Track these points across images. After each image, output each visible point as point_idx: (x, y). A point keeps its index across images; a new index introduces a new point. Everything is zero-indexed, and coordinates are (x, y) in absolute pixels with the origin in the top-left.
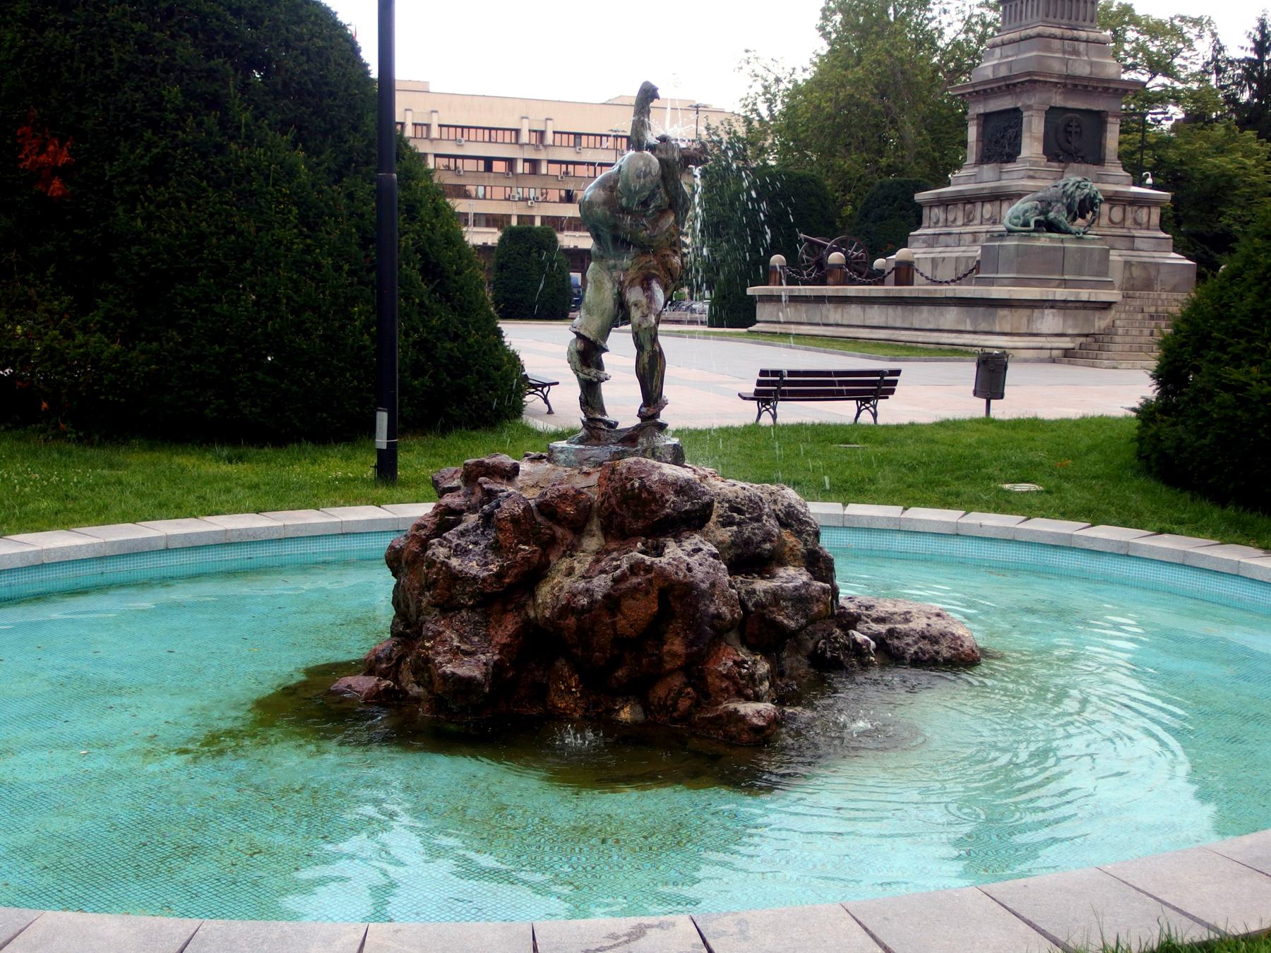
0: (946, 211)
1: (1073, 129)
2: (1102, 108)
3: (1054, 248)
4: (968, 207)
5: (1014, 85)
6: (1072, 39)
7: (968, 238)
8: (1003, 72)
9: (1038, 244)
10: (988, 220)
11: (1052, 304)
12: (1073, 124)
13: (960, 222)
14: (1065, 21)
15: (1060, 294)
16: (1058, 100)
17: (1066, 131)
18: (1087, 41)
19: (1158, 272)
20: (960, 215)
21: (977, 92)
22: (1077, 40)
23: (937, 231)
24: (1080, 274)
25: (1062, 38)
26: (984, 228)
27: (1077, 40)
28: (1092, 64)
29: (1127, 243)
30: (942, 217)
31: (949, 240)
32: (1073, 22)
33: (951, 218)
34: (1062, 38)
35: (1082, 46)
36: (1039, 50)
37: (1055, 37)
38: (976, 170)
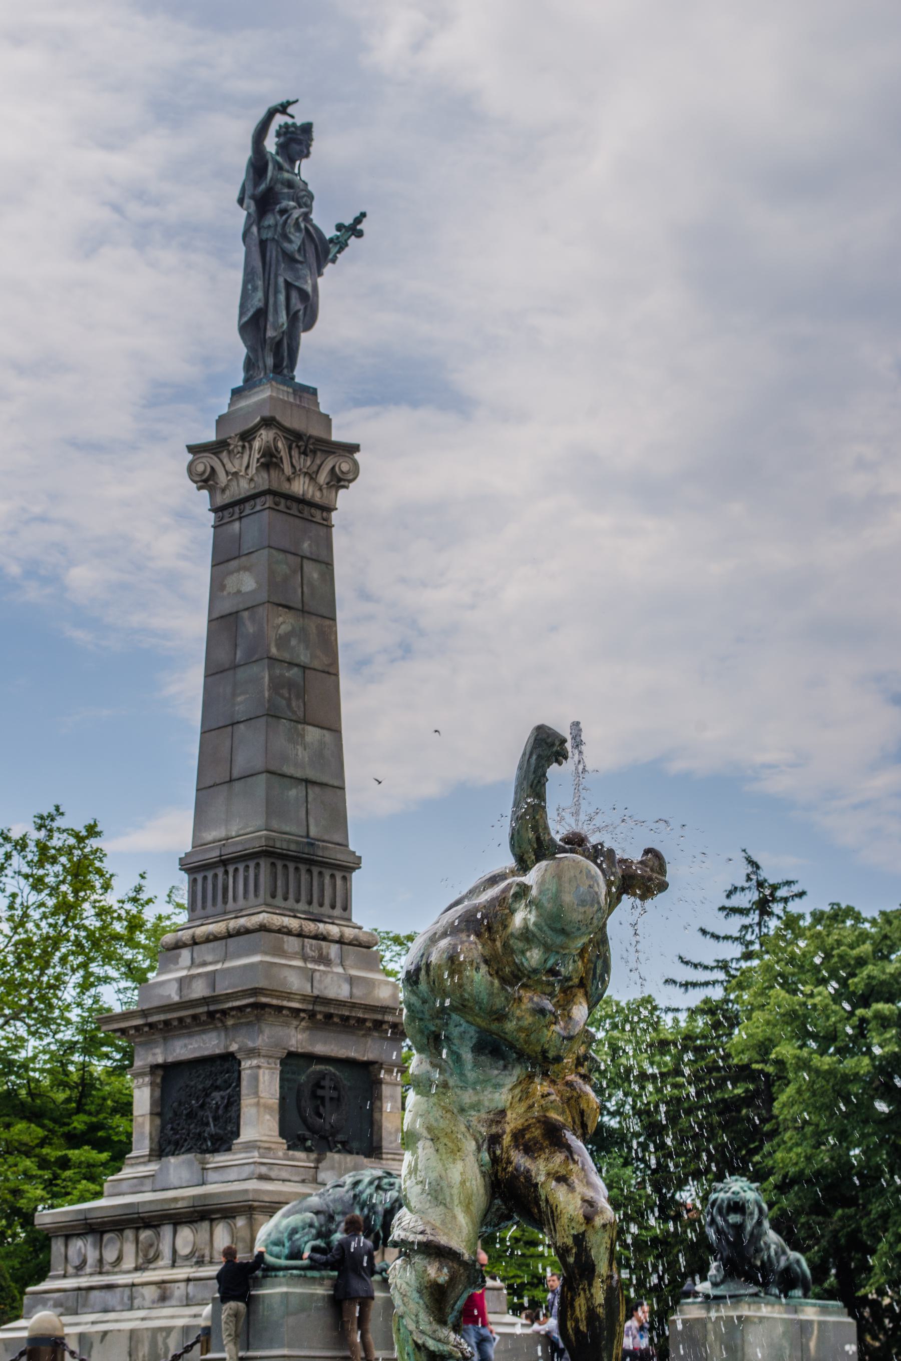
0: (100, 1245)
1: (328, 1093)
2: (369, 1056)
4: (145, 1235)
5: (224, 1012)
7: (150, 1293)
8: (199, 990)
10: (187, 1258)
12: (326, 1083)
13: (129, 1263)
14: (302, 906)
16: (297, 1038)
17: (314, 1096)
18: (341, 941)
20: (129, 1249)
21: (151, 1025)
22: (324, 938)
23: (84, 1282)
25: (300, 935)
26: (182, 1273)
28: (351, 980)
30: (92, 1255)
31: (111, 1298)
32: (315, 908)
33: (110, 1255)
34: (300, 935)
36: (265, 953)
37: (289, 933)
38: (153, 1167)
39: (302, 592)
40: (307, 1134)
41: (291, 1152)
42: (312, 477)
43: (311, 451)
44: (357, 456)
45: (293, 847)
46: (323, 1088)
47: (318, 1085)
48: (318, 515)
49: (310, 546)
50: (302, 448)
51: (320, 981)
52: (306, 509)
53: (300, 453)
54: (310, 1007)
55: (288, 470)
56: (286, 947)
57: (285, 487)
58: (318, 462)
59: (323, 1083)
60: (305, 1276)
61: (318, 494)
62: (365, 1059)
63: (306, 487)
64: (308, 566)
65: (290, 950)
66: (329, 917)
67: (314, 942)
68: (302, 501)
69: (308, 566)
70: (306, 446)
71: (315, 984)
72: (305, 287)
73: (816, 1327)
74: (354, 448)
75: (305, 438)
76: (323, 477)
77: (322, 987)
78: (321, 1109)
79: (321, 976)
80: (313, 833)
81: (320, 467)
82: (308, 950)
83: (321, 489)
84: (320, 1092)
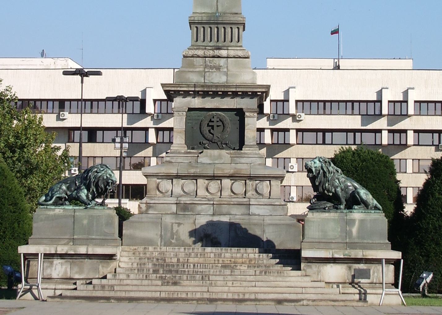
3: (66, 217)
6: (213, 57)
9: (51, 213)
11: (62, 256)
12: (215, 119)
15: (61, 250)
16: (197, 102)
17: (208, 125)
19: (264, 231)
22: (219, 57)
24: (89, 234)
27: (219, 57)
29: (242, 210)
32: (220, 44)
35: (222, 62)
37: (198, 57)
40: (205, 142)
41: (189, 151)
45: (205, 18)
46: (213, 122)
47: (211, 121)
51: (209, 77)
54: (193, 89)
56: (195, 63)
59: (212, 120)
60: (47, 208)
62: (235, 108)
65: (197, 64)
66: (224, 46)
67: (211, 59)
71: (206, 78)
73: (357, 222)
77: (210, 78)
78: (212, 131)
79: (209, 74)
80: (220, 10)
82: (208, 63)
84: (211, 124)
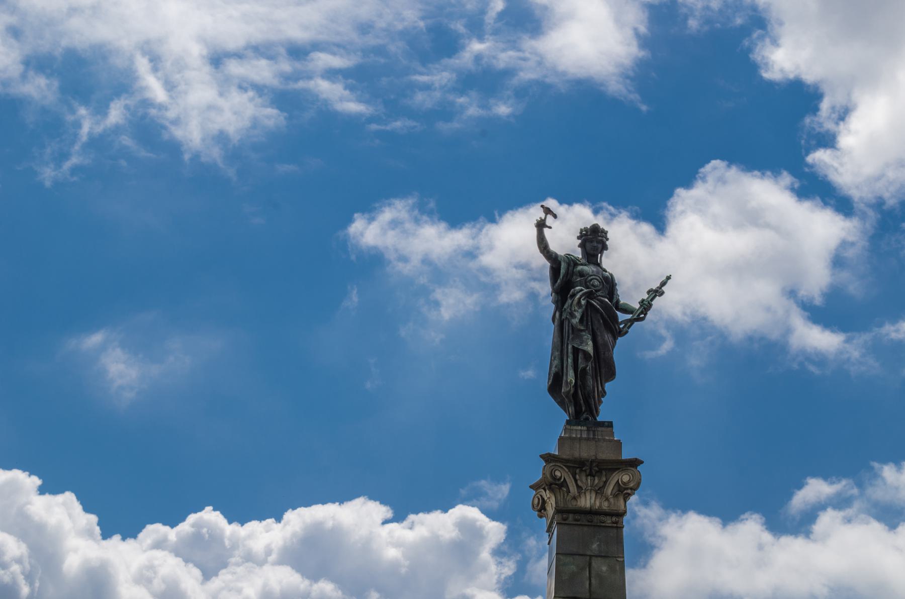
39: (590, 584)
42: (599, 491)
43: (597, 472)
44: (639, 468)
48: (608, 521)
49: (599, 546)
50: (588, 471)
52: (596, 519)
53: (587, 476)
55: (573, 489)
57: (572, 505)
58: (604, 479)
61: (606, 504)
63: (593, 501)
64: (596, 563)
68: (591, 512)
69: (596, 563)
70: (591, 470)
72: (585, 348)
74: (634, 463)
75: (588, 464)
76: (609, 490)
81: (605, 483)
83: (607, 499)
